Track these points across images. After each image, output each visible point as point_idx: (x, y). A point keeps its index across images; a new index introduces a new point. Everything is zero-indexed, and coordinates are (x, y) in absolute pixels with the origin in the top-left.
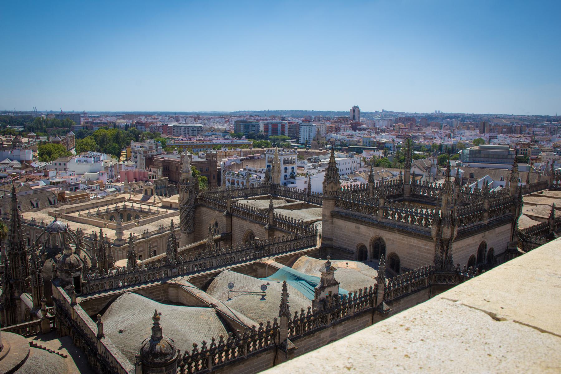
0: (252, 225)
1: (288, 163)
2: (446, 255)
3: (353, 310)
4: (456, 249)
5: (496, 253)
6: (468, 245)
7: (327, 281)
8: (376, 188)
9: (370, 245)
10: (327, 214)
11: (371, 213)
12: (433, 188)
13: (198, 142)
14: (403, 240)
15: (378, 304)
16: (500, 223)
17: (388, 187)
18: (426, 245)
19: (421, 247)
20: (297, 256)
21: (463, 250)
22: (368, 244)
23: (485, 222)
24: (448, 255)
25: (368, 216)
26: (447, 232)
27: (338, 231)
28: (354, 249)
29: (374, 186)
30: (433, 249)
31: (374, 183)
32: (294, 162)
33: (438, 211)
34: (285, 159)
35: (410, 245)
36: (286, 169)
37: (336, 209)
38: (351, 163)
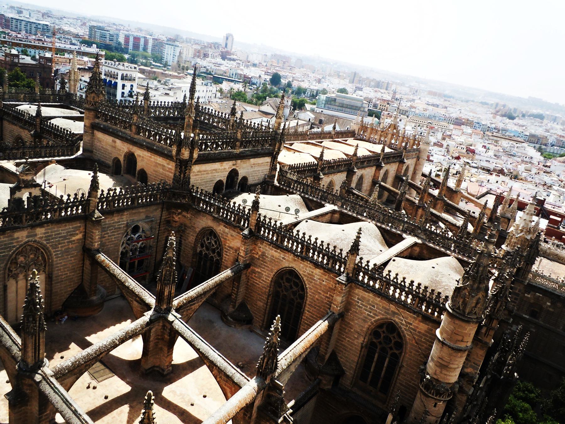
0: (21, 130)
1: (126, 80)
2: (184, 176)
3: (57, 214)
4: (198, 172)
5: (251, 181)
6: (214, 170)
7: (24, 181)
8: (152, 108)
9: (124, 160)
10: (87, 125)
11: (125, 128)
12: (213, 116)
13: (37, 42)
14: (151, 157)
15: (91, 211)
16: (256, 155)
17: (167, 108)
18: (168, 164)
19: (164, 166)
20: (47, 163)
21: (207, 174)
22: (122, 159)
23: (237, 151)
24: (186, 175)
25: (123, 130)
26: (186, 154)
27: (98, 144)
28: (110, 163)
29: (150, 104)
30: (174, 168)
31: (150, 102)
32: (134, 80)
33: (180, 133)
34: (122, 75)
35: (156, 163)
36: (124, 86)
37: (97, 121)
38: (205, 91)
